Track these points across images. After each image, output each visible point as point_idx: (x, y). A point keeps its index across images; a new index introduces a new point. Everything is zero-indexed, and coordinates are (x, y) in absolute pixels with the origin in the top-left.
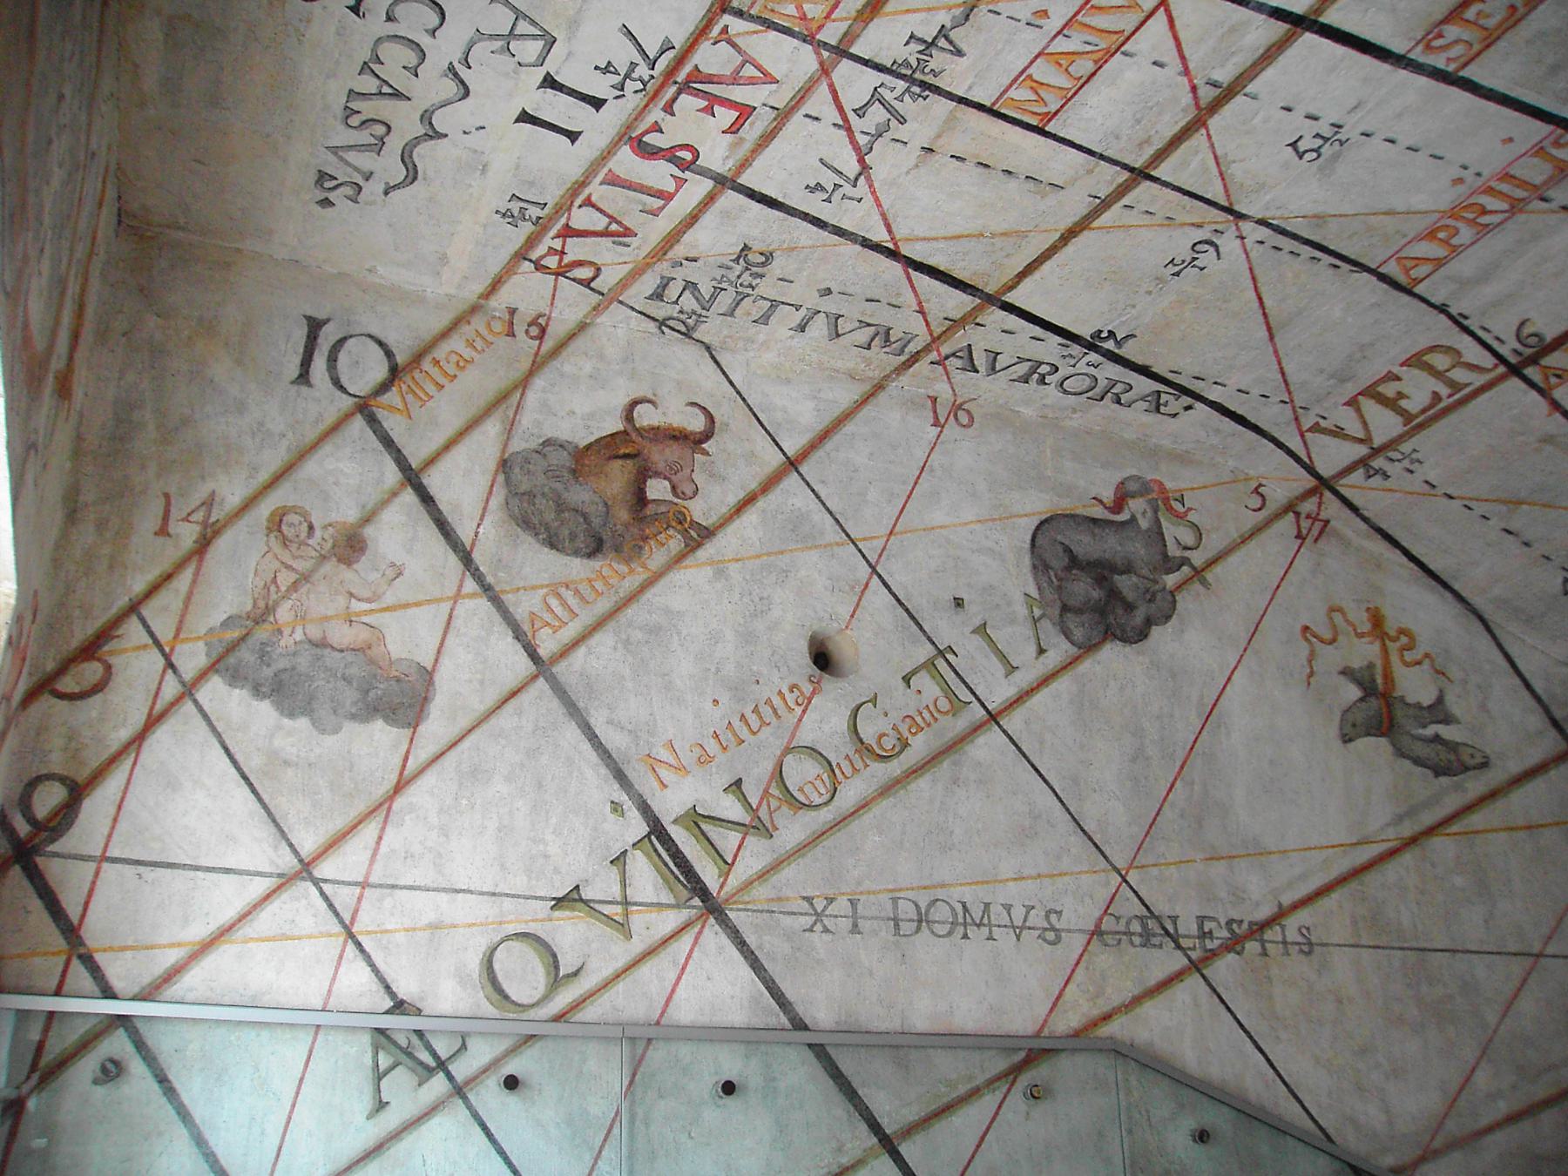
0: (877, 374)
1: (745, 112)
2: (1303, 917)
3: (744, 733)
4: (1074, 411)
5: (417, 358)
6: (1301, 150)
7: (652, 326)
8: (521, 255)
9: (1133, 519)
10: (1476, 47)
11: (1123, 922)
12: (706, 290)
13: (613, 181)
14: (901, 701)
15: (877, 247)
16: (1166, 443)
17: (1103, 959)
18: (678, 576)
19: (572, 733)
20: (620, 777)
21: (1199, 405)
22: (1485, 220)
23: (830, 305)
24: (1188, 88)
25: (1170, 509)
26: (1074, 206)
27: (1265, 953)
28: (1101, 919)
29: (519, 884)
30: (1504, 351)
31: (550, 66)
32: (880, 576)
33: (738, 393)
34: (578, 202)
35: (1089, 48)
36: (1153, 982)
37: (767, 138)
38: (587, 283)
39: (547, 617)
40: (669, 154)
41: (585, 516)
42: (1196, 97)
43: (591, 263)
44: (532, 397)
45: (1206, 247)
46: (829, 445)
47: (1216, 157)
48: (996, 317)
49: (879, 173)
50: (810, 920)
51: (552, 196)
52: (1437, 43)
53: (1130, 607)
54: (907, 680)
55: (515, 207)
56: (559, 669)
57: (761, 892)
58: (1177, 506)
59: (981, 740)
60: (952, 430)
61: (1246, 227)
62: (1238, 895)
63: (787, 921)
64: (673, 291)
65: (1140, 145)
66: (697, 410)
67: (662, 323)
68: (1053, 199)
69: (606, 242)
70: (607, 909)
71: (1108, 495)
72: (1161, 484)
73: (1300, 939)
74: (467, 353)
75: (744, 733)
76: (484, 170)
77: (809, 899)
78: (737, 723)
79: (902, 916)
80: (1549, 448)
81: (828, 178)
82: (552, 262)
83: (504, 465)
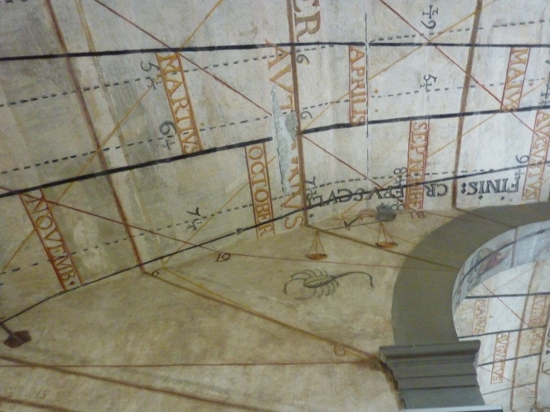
6: (431, 78)
10: (413, 130)
22: (355, 84)
24: (479, 82)
26: (486, 21)
30: (302, 48)
35: (513, 80)
42: (475, 80)
47: (454, 63)
52: (424, 126)
65: (480, 56)
80: (251, 28)
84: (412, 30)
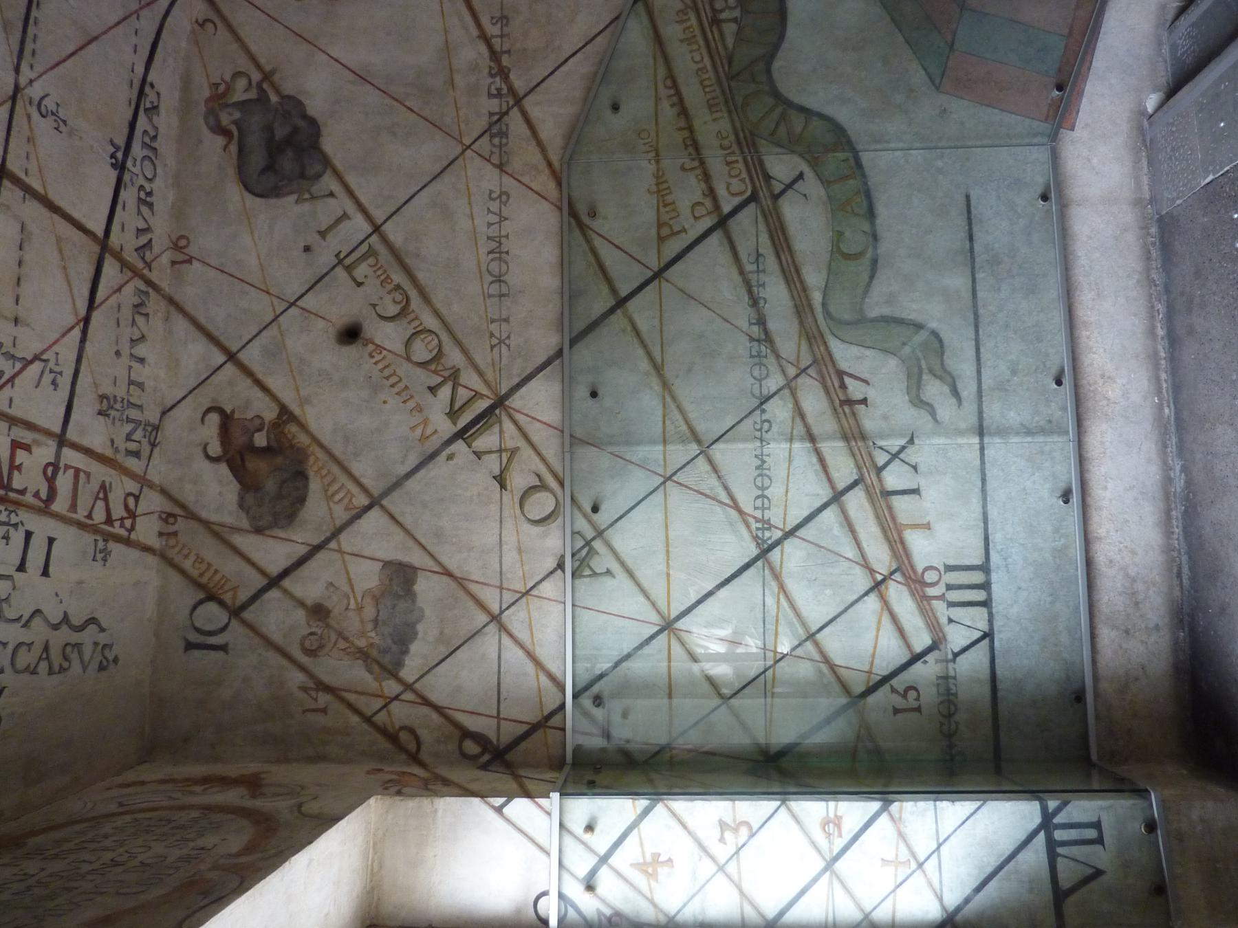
0: (163, 304)
1: (16, 445)
2: (485, 21)
3: (401, 385)
4: (166, 165)
5: (200, 586)
7: (156, 450)
8: (127, 542)
9: (235, 123)
11: (494, 150)
12: (128, 427)
13: (73, 507)
14: (372, 289)
15: (84, 332)
16: (177, 95)
17: (516, 164)
18: (313, 425)
19: (411, 484)
20: (433, 456)
21: (149, 79)
23: (126, 351)
25: (224, 95)
27: (508, 52)
28: (493, 165)
29: (494, 508)
31: (11, 571)
32: (296, 300)
33: (190, 392)
34: (90, 522)
36: (528, 132)
37: (30, 426)
38: (137, 498)
39: (346, 501)
40: (51, 481)
41: (284, 482)
43: (125, 499)
44: (214, 517)
45: (43, 108)
46: (216, 333)
48: (115, 240)
49: (37, 347)
50: (504, 347)
51: (88, 538)
53: (296, 130)
54: (359, 284)
55: (99, 556)
56: (376, 493)
57: (490, 375)
58: (222, 88)
59: (392, 237)
60: (193, 250)
61: (23, 81)
62: (474, 68)
63: (504, 361)
64: (132, 446)
66: (206, 418)
67: (153, 445)
68: (33, 228)
69: (111, 496)
70: (505, 460)
71: (220, 141)
72: (207, 101)
73: (499, 25)
74: (192, 558)
75: (401, 385)
76: (80, 583)
77: (492, 347)
78: (396, 389)
79: (497, 293)
81: (48, 377)
82: (128, 523)
83: (259, 531)
84: (41, 70)
